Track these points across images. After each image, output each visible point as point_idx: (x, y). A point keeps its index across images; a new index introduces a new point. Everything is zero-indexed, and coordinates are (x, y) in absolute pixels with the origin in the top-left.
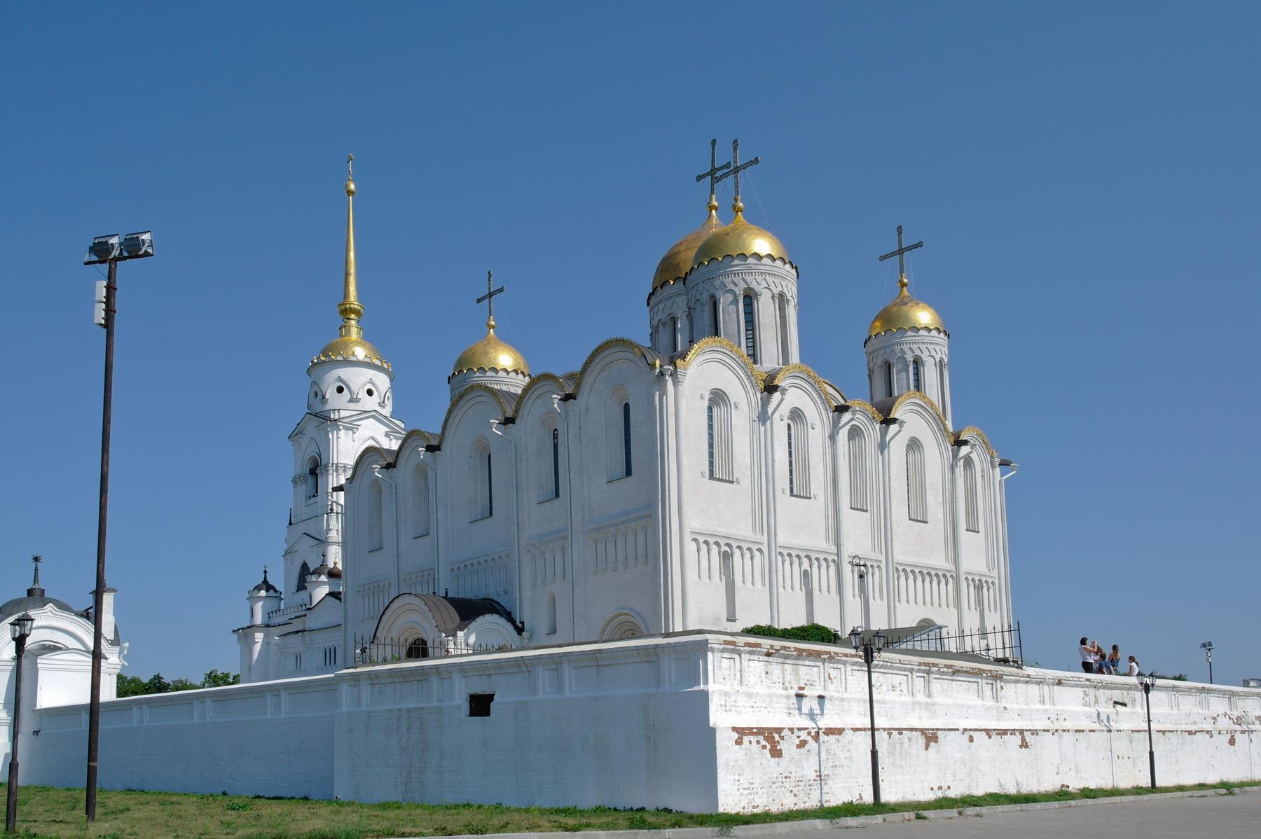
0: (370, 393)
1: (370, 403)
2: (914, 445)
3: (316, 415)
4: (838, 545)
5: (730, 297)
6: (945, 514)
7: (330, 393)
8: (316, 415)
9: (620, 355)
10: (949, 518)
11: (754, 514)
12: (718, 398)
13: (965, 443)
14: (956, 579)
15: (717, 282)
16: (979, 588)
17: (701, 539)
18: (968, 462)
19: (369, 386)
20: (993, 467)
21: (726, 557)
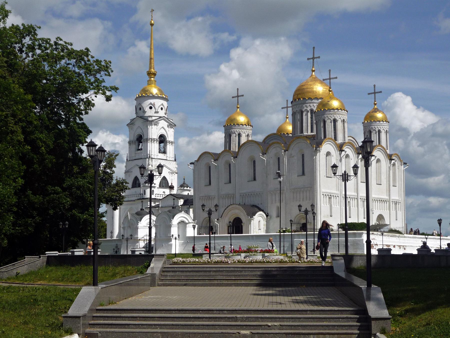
0: (162, 109)
1: (162, 113)
2: (378, 161)
3: (141, 117)
4: (358, 194)
5: (330, 121)
6: (387, 181)
7: (147, 109)
8: (141, 117)
9: (302, 141)
10: (388, 182)
11: (336, 186)
12: (328, 154)
13: (393, 159)
14: (389, 201)
15: (325, 116)
16: (396, 203)
17: (324, 194)
18: (394, 165)
19: (162, 106)
20: (401, 165)
21: (330, 198)
